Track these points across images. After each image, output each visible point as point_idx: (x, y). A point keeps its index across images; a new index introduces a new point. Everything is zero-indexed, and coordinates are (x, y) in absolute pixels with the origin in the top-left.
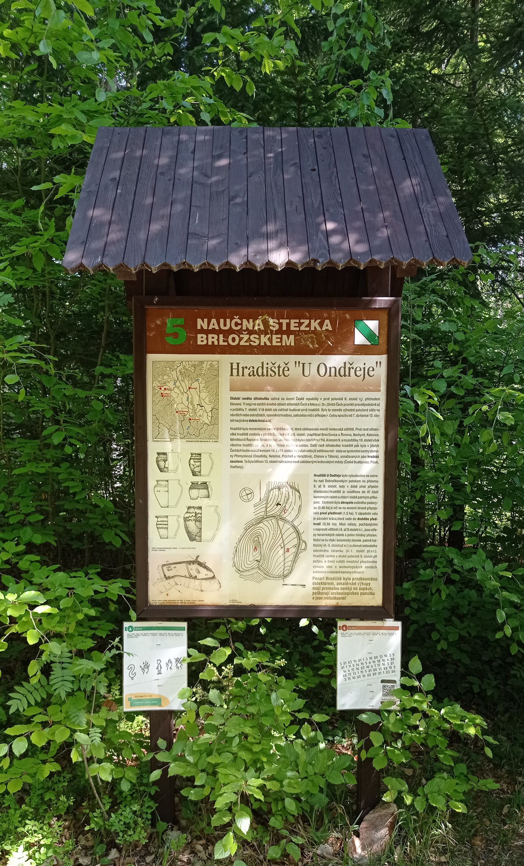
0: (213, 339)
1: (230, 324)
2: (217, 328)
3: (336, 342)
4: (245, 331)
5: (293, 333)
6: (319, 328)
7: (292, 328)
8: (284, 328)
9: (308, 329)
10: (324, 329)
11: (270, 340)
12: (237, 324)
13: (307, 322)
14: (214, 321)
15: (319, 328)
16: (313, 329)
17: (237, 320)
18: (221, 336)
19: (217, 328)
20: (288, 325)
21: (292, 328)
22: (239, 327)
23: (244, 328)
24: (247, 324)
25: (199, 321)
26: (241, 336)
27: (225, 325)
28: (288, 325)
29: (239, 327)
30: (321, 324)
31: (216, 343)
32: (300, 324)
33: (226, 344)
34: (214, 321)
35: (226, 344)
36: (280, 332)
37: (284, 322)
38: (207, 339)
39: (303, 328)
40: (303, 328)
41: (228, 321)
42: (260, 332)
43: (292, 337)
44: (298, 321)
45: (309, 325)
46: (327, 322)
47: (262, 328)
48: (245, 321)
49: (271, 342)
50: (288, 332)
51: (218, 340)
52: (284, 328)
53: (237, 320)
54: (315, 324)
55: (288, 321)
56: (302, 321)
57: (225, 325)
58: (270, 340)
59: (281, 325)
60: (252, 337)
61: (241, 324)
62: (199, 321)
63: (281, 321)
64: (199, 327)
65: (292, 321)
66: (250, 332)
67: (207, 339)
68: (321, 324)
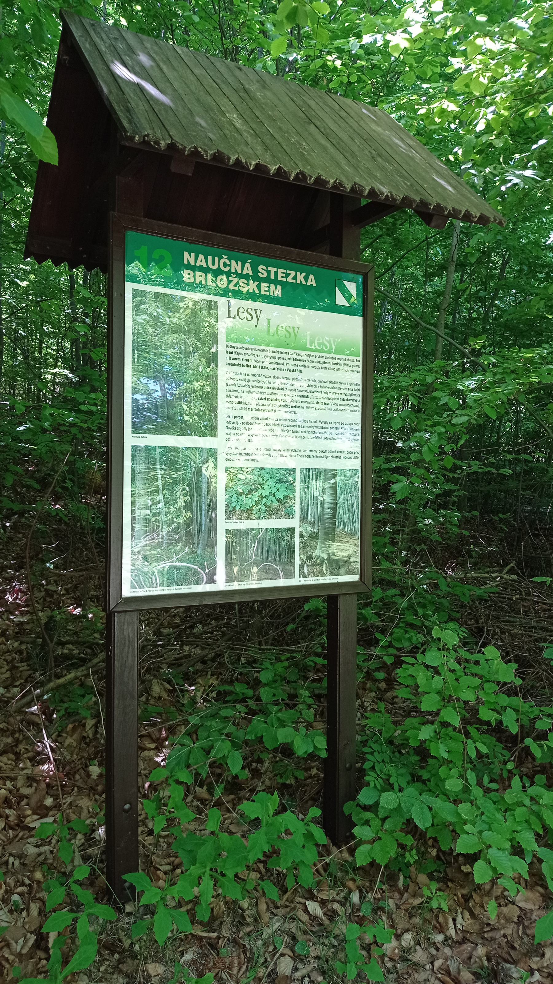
0: (199, 277)
1: (219, 263)
2: (205, 266)
3: (318, 299)
4: (234, 273)
6: (304, 283)
7: (280, 278)
8: (272, 277)
9: (294, 281)
11: (259, 287)
12: (225, 265)
13: (293, 273)
14: (201, 257)
16: (298, 282)
17: (225, 260)
19: (205, 266)
20: (276, 273)
21: (280, 278)
22: (227, 269)
24: (236, 266)
25: (186, 254)
26: (230, 278)
27: (213, 264)
28: (276, 273)
29: (227, 269)
34: (201, 257)
36: (267, 280)
37: (272, 270)
38: (194, 276)
40: (289, 279)
41: (216, 259)
42: (246, 277)
43: (279, 287)
45: (295, 278)
46: (311, 277)
48: (233, 262)
49: (260, 291)
50: (276, 282)
51: (206, 279)
52: (272, 277)
53: (225, 260)
54: (300, 277)
55: (275, 269)
56: (289, 272)
57: (213, 264)
58: (259, 287)
59: (268, 272)
61: (230, 265)
62: (186, 254)
63: (269, 268)
64: (186, 262)
65: (280, 271)
67: (194, 276)
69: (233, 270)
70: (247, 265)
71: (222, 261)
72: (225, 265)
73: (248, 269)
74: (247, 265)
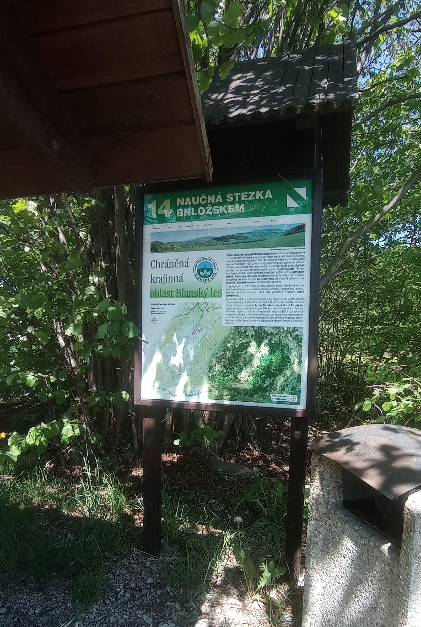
1: (200, 200)
4: (209, 204)
5: (243, 202)
6: (262, 197)
8: (237, 199)
9: (254, 198)
10: (266, 197)
12: (203, 200)
13: (253, 193)
14: (188, 199)
15: (262, 197)
16: (258, 198)
18: (193, 209)
21: (243, 199)
22: (205, 201)
23: (209, 202)
24: (211, 199)
25: (179, 200)
26: (207, 208)
27: (196, 201)
28: (240, 197)
29: (205, 201)
30: (264, 194)
31: (190, 215)
32: (249, 195)
33: (196, 214)
34: (188, 199)
35: (196, 214)
37: (237, 195)
38: (183, 212)
39: (250, 198)
40: (250, 198)
41: (198, 198)
42: (219, 204)
44: (247, 193)
45: (255, 196)
46: (269, 192)
47: (221, 201)
48: (209, 197)
52: (237, 199)
54: (259, 195)
55: (240, 194)
56: (250, 193)
57: (196, 201)
59: (234, 197)
60: (214, 209)
61: (207, 199)
62: (179, 200)
63: (234, 194)
65: (243, 194)
66: (213, 205)
67: (183, 212)
68: (264, 194)
69: (209, 202)
70: (219, 196)
71: (201, 198)
72: (203, 200)
73: (219, 198)
74: (219, 196)
